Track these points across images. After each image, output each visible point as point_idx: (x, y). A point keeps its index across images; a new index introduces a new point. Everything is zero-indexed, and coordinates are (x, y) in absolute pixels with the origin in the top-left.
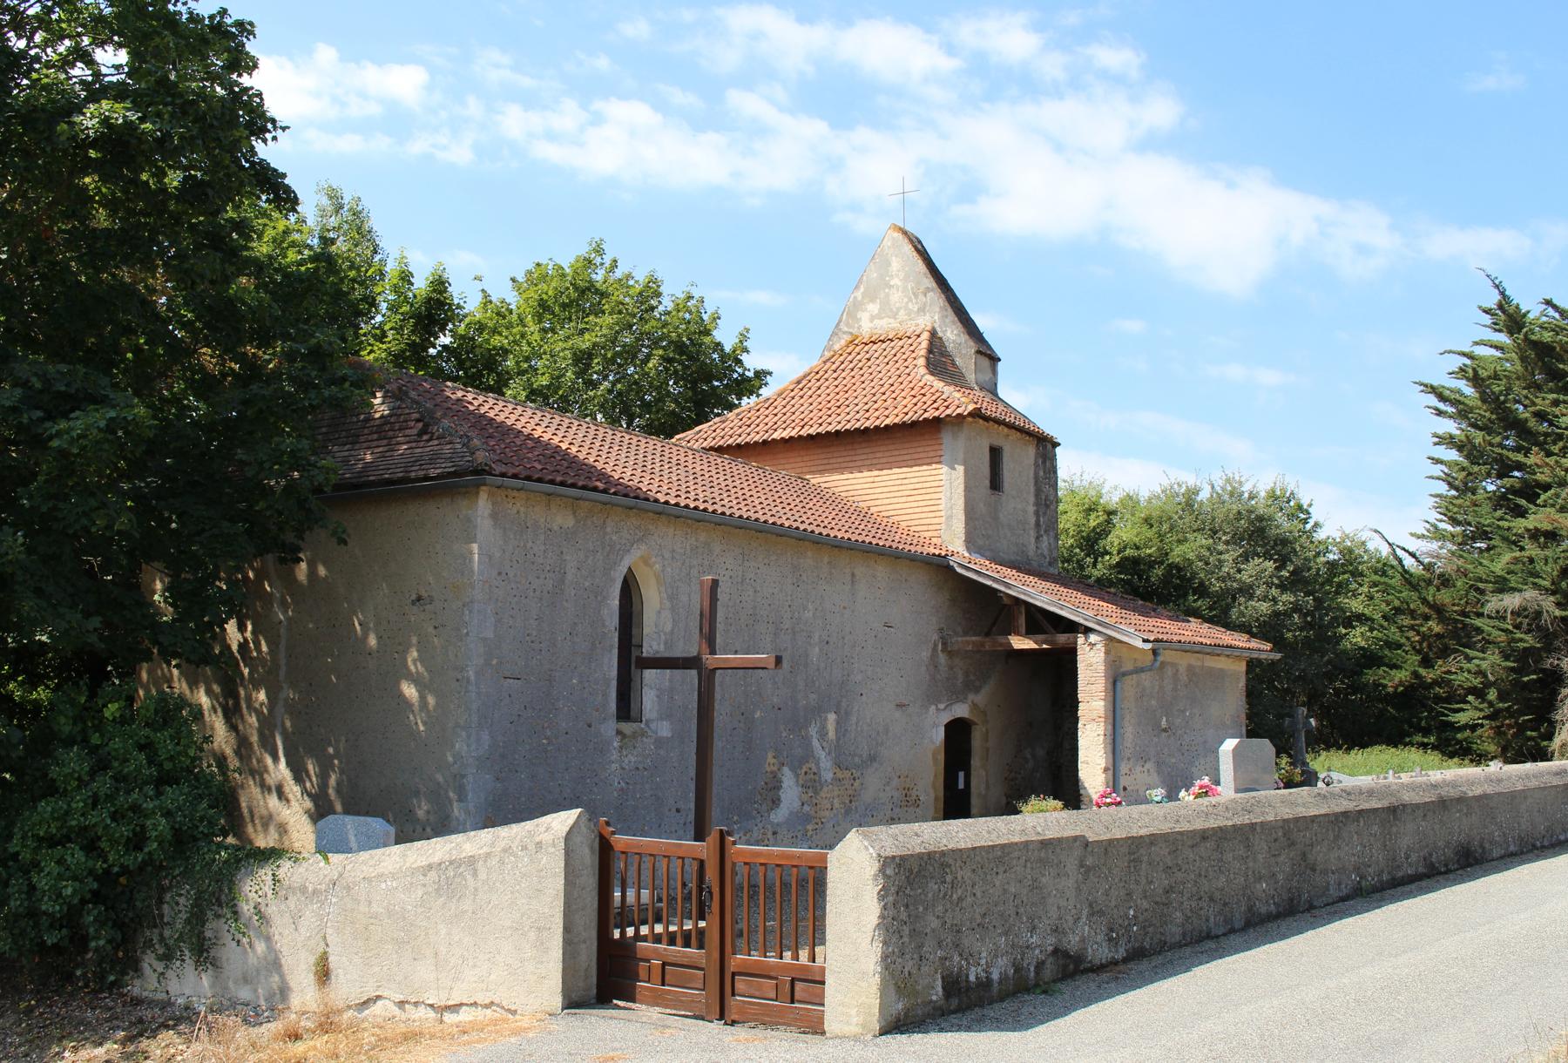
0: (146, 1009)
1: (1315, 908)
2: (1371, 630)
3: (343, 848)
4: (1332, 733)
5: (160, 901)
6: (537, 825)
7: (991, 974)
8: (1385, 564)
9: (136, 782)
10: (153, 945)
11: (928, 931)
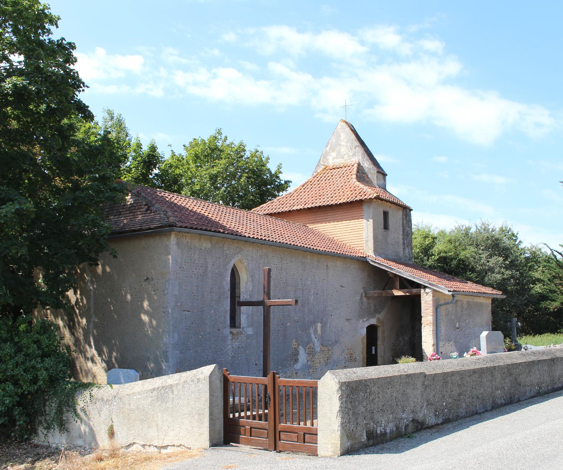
0: (40, 449)
1: (521, 401)
2: (544, 285)
3: (118, 382)
4: (528, 328)
5: (45, 405)
6: (198, 372)
7: (386, 430)
8: (549, 258)
9: (33, 356)
10: (42, 423)
11: (360, 412)
